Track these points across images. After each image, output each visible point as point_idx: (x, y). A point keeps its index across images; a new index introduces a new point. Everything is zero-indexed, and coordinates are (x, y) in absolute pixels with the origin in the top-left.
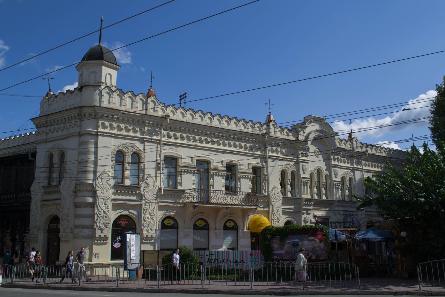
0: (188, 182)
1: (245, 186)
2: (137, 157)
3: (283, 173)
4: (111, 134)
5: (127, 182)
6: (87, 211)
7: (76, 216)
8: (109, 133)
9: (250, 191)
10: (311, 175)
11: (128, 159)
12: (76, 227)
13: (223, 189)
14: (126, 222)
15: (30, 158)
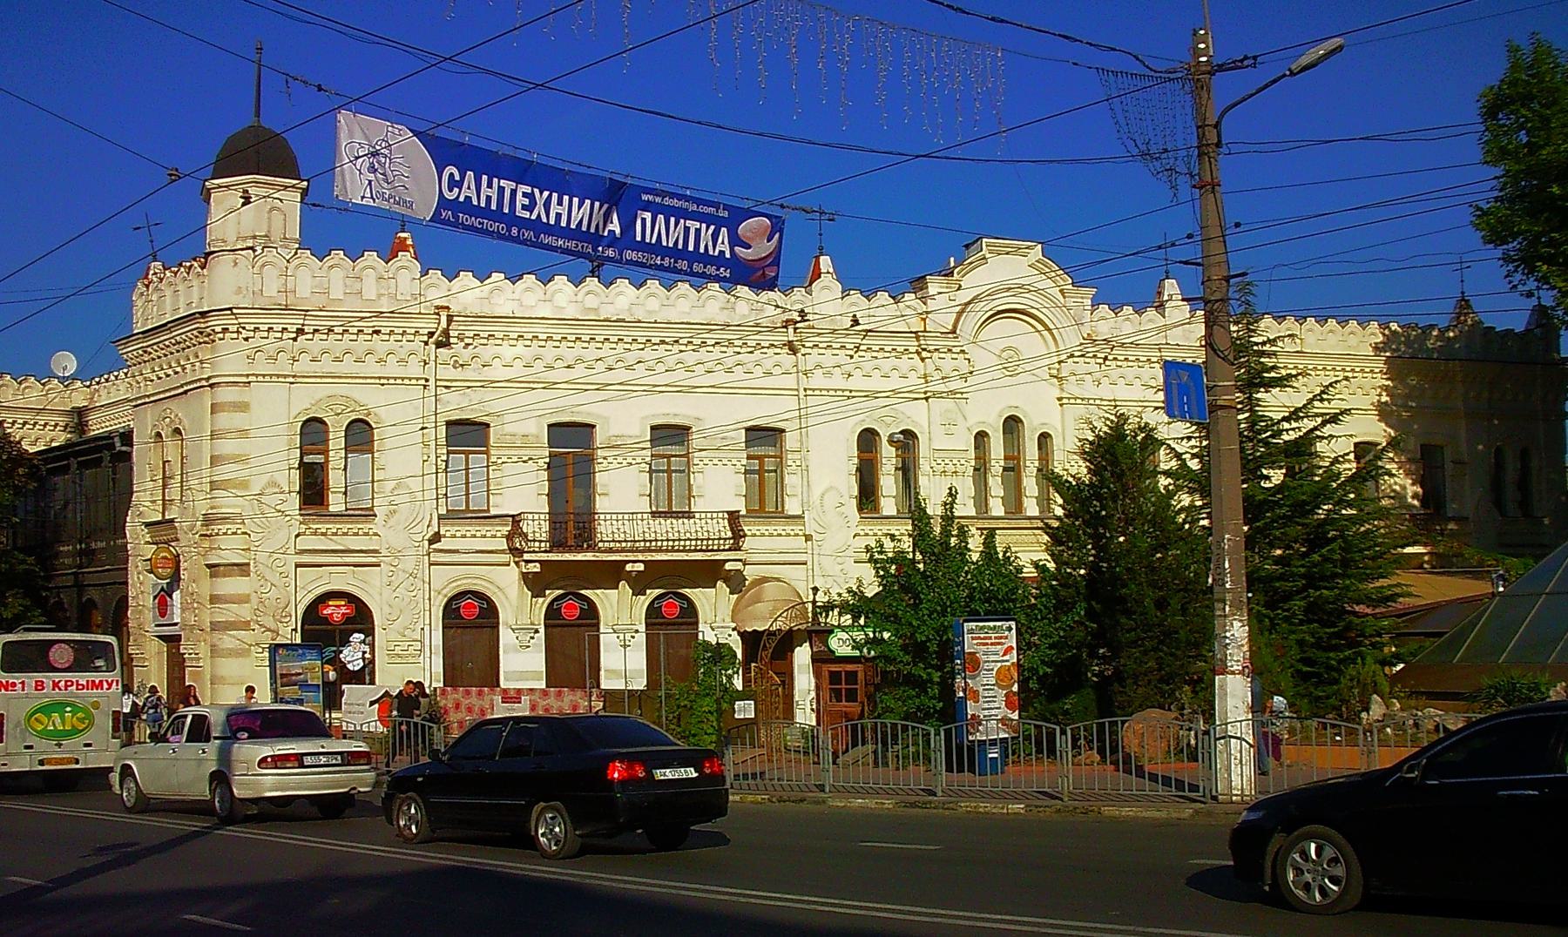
0: (523, 490)
1: (719, 486)
2: (360, 435)
3: (868, 439)
4: (285, 376)
5: (336, 503)
6: (230, 585)
7: (214, 599)
8: (278, 376)
9: (740, 506)
10: (981, 437)
11: (337, 441)
12: (215, 627)
13: (644, 505)
14: (344, 610)
15: (119, 447)
